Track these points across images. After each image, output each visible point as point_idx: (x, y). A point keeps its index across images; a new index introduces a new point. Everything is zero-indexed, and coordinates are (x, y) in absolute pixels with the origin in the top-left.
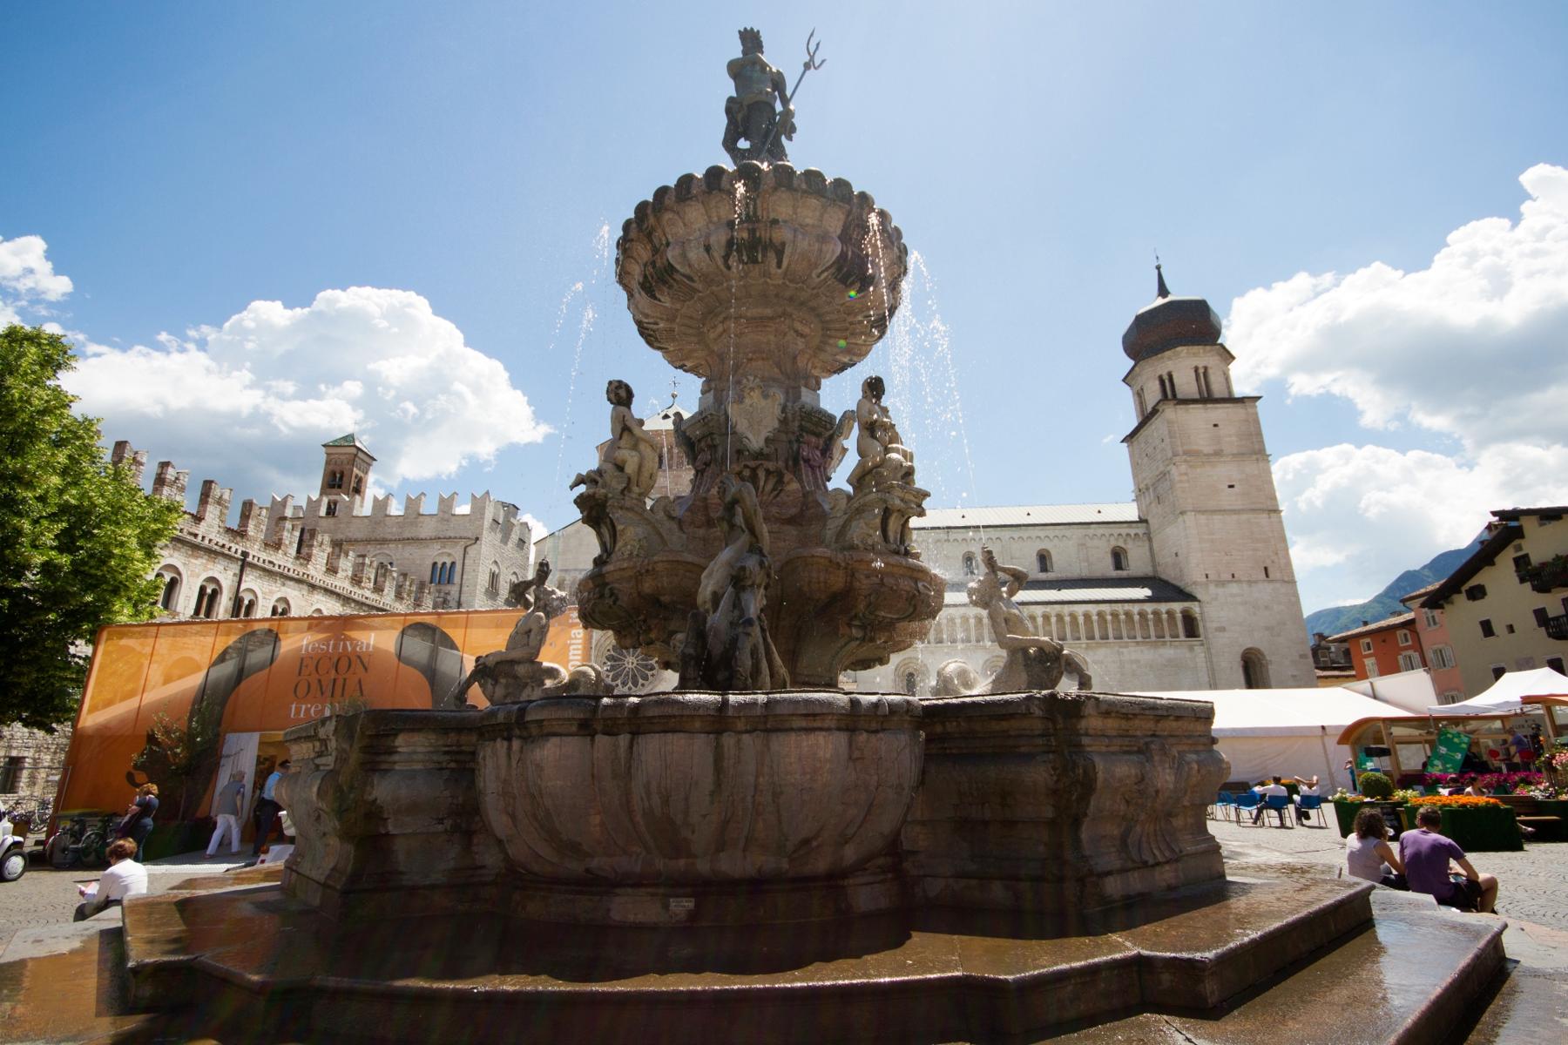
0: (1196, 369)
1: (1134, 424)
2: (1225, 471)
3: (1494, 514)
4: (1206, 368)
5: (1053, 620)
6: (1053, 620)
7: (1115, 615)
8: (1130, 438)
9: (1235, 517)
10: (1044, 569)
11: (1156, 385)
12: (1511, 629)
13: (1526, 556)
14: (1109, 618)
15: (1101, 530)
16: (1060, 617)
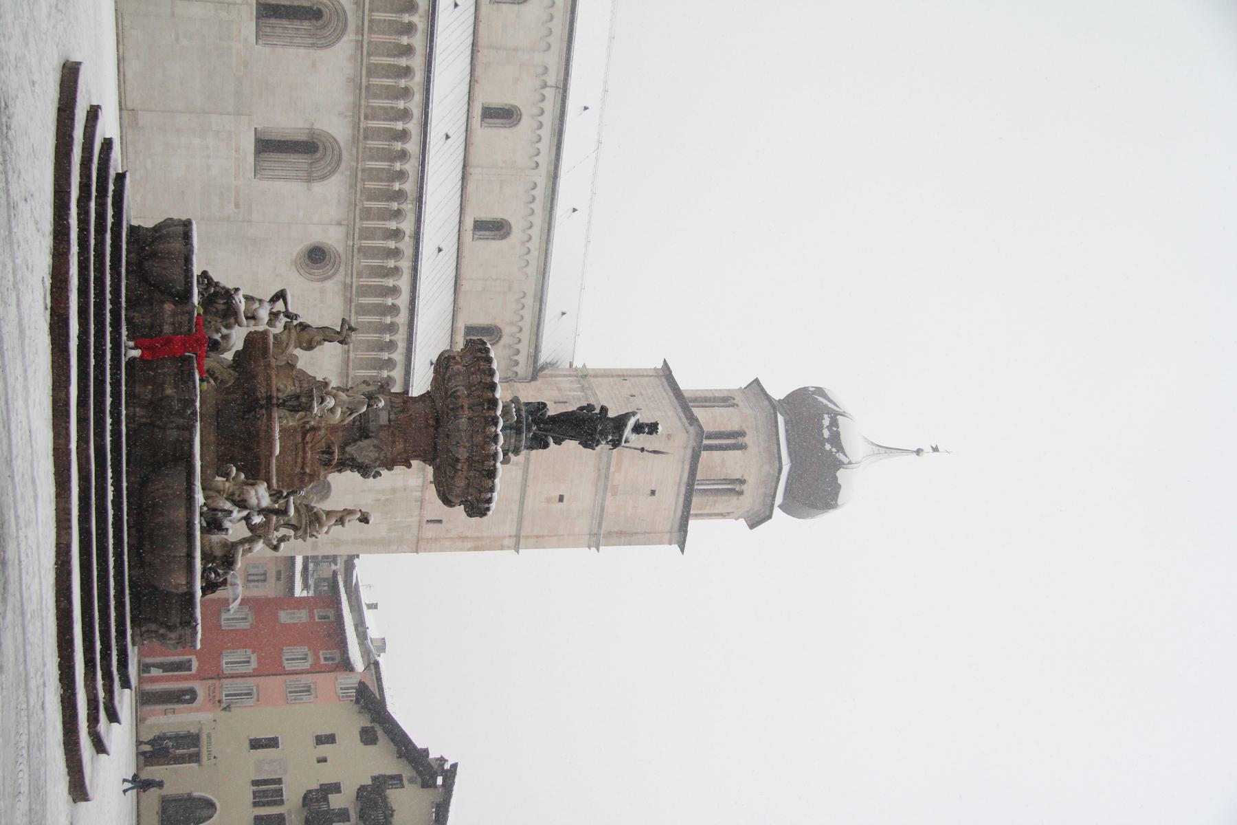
0: (742, 482)
1: (683, 385)
2: (582, 494)
3: (454, 766)
4: (741, 493)
5: (392, 244)
6: (392, 244)
7: (392, 328)
8: (666, 374)
9: (517, 496)
10: (480, 226)
11: (734, 426)
12: (323, 760)
13: (403, 786)
14: (388, 320)
15: (528, 314)
16: (396, 253)
